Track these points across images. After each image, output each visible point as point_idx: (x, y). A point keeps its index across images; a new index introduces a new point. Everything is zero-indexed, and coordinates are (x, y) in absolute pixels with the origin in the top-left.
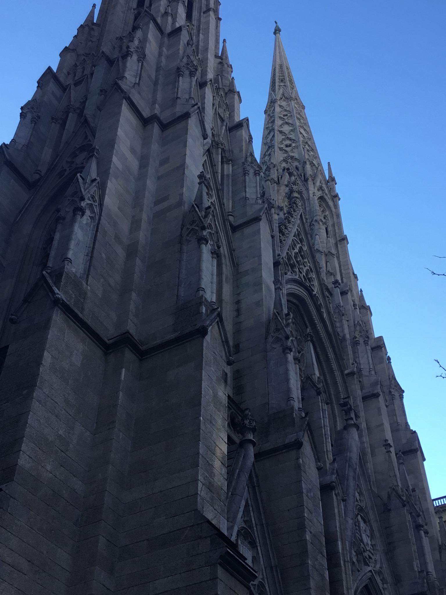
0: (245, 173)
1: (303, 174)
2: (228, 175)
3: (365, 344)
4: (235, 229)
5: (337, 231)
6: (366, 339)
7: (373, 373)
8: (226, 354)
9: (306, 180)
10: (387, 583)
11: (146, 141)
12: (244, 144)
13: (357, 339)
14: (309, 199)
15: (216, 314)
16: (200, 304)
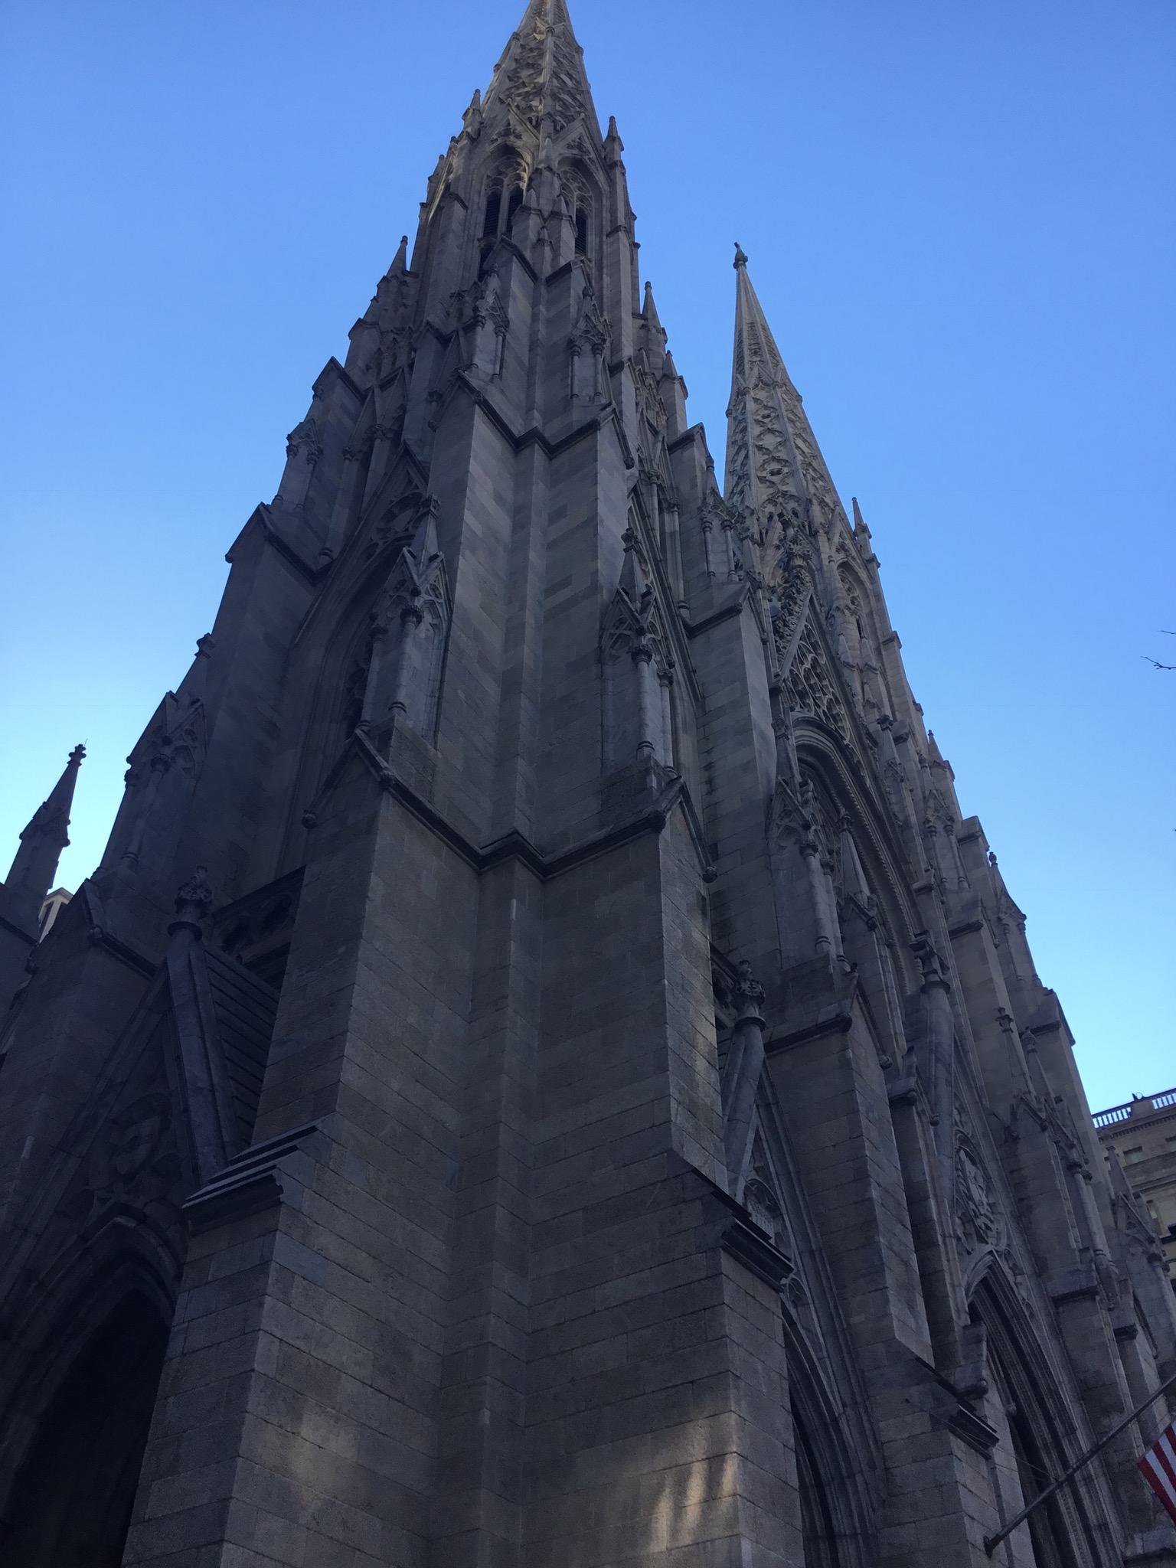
0: (705, 527)
1: (806, 523)
2: (673, 534)
3: (947, 832)
4: (692, 632)
5: (878, 625)
6: (949, 823)
7: (966, 885)
8: (700, 862)
9: (814, 534)
10: (1022, 1273)
11: (521, 480)
12: (698, 473)
13: (931, 824)
14: (821, 569)
15: (676, 788)
16: (647, 771)
